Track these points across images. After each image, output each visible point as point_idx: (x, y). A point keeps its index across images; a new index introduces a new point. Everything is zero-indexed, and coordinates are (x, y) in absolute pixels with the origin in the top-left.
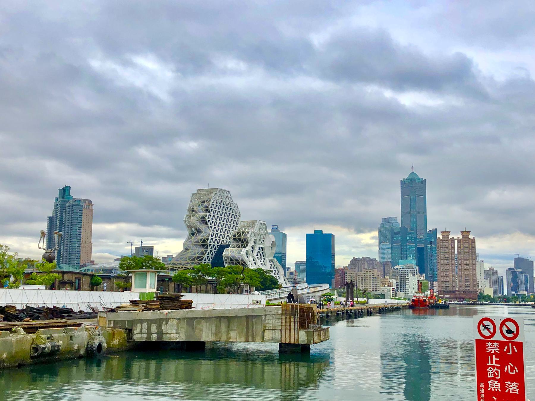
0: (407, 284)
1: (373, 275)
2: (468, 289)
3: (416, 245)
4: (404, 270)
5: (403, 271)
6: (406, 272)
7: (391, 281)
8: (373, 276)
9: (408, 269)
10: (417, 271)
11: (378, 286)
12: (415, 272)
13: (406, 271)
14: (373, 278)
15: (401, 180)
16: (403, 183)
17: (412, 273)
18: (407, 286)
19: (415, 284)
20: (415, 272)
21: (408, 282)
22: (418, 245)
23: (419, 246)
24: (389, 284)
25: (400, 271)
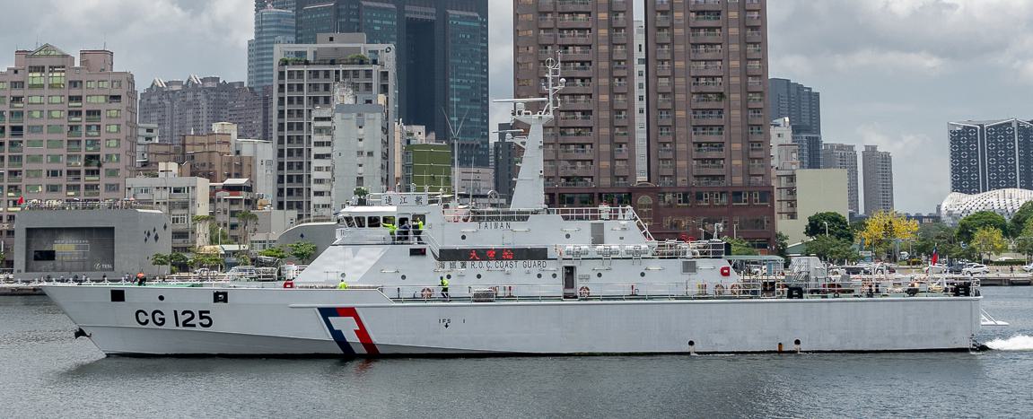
0: (317, 157)
1: (75, 92)
2: (714, 177)
3: (401, 10)
4: (305, 69)
5: (300, 74)
7: (247, 151)
8: (79, 99)
9: (333, 63)
10: (385, 75)
11: (113, 173)
12: (375, 81)
13: (316, 74)
14: (78, 113)
17: (355, 87)
18: (319, 169)
19: (370, 154)
20: (375, 81)
21: (329, 144)
22: (407, 8)
23: (411, 12)
24: (229, 164)
25: (282, 74)
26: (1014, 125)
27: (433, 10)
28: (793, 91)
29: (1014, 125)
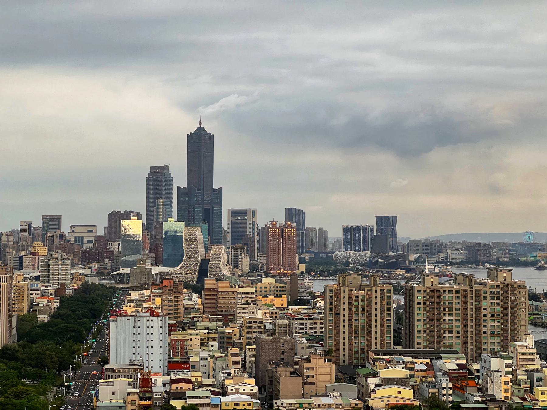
3: (203, 207)
6: (237, 251)
15: (188, 135)
16: (190, 137)
26: (361, 227)
27: (210, 206)
28: (297, 212)
29: (361, 227)
